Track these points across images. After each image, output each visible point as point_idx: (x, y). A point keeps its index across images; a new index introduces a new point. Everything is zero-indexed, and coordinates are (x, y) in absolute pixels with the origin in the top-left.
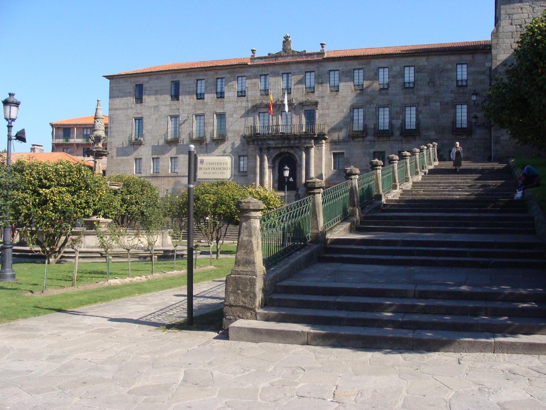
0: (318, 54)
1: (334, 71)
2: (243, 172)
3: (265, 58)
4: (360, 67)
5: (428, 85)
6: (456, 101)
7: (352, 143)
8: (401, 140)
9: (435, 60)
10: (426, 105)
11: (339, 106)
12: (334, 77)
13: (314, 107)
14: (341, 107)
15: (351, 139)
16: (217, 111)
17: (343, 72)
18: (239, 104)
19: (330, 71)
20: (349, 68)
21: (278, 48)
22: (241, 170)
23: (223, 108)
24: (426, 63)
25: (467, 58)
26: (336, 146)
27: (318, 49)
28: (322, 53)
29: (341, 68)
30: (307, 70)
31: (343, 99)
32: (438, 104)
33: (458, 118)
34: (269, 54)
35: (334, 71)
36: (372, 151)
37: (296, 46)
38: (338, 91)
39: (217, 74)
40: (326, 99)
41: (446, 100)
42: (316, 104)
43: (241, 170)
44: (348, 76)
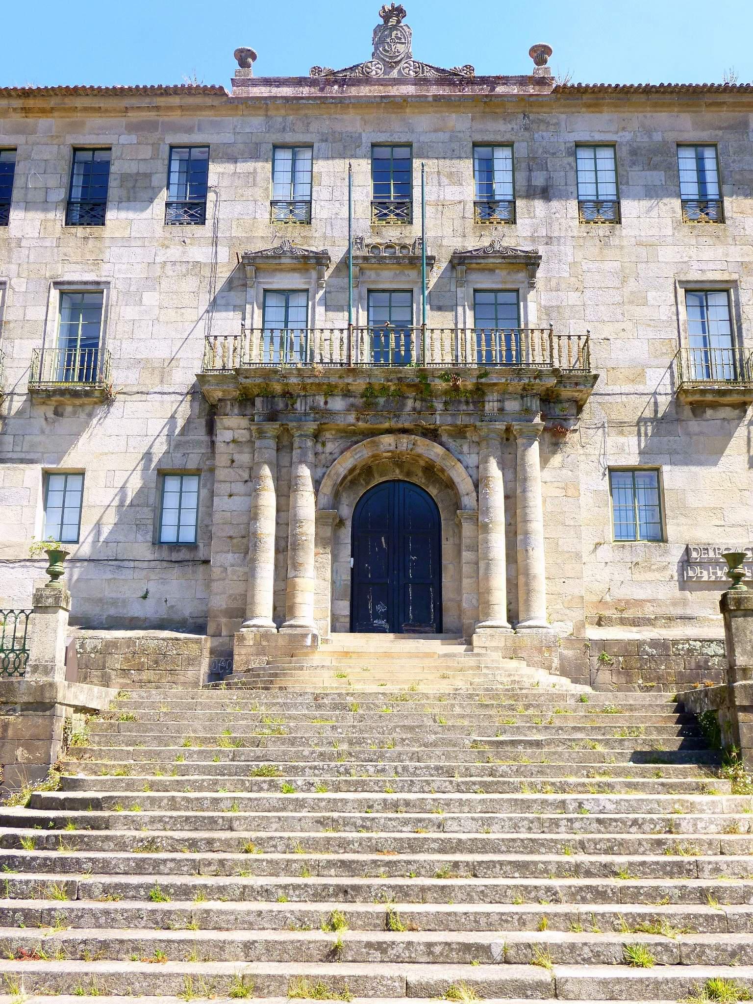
0: (523, 81)
1: (595, 146)
2: (176, 546)
3: (300, 82)
4: (704, 136)
11: (624, 280)
12: (596, 174)
13: (522, 276)
14: (632, 285)
15: (687, 411)
16: (67, 278)
17: (634, 152)
18: (174, 252)
19: (578, 145)
20: (658, 137)
22: (168, 535)
23: (97, 262)
26: (622, 440)
27: (528, 68)
29: (623, 137)
30: (478, 138)
31: (643, 251)
34: (316, 70)
35: (595, 146)
39: (75, 127)
40: (567, 251)
42: (529, 263)
43: (168, 535)
44: (655, 168)
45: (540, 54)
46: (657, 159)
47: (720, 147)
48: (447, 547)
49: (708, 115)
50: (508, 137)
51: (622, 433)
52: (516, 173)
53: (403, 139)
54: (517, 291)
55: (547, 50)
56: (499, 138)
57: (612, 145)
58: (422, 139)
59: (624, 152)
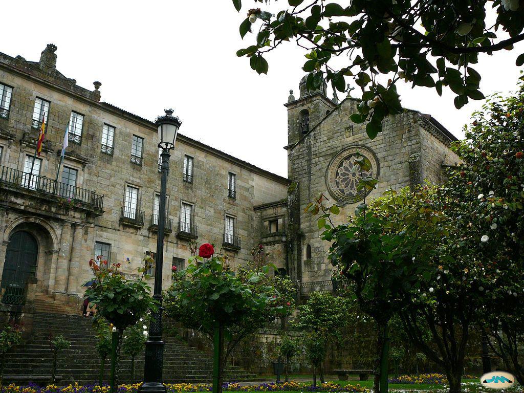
1: (109, 126)
5: (205, 185)
6: (227, 212)
7: (122, 233)
8: (177, 244)
9: (213, 161)
10: (202, 208)
13: (80, 166)
17: (121, 133)
19: (105, 124)
20: (128, 130)
21: (33, 55)
24: (204, 160)
25: (236, 170)
27: (92, 88)
28: (97, 95)
32: (212, 210)
33: (227, 232)
36: (145, 250)
37: (64, 66)
38: (111, 155)
41: (220, 207)
45: (97, 84)
46: (126, 138)
47: (145, 140)
48: (41, 260)
49: (142, 129)
50: (83, 113)
51: (102, 230)
52: (84, 127)
53: (49, 99)
54: (77, 170)
55: (100, 84)
56: (81, 112)
57: (115, 128)
58: (55, 102)
59: (117, 132)
